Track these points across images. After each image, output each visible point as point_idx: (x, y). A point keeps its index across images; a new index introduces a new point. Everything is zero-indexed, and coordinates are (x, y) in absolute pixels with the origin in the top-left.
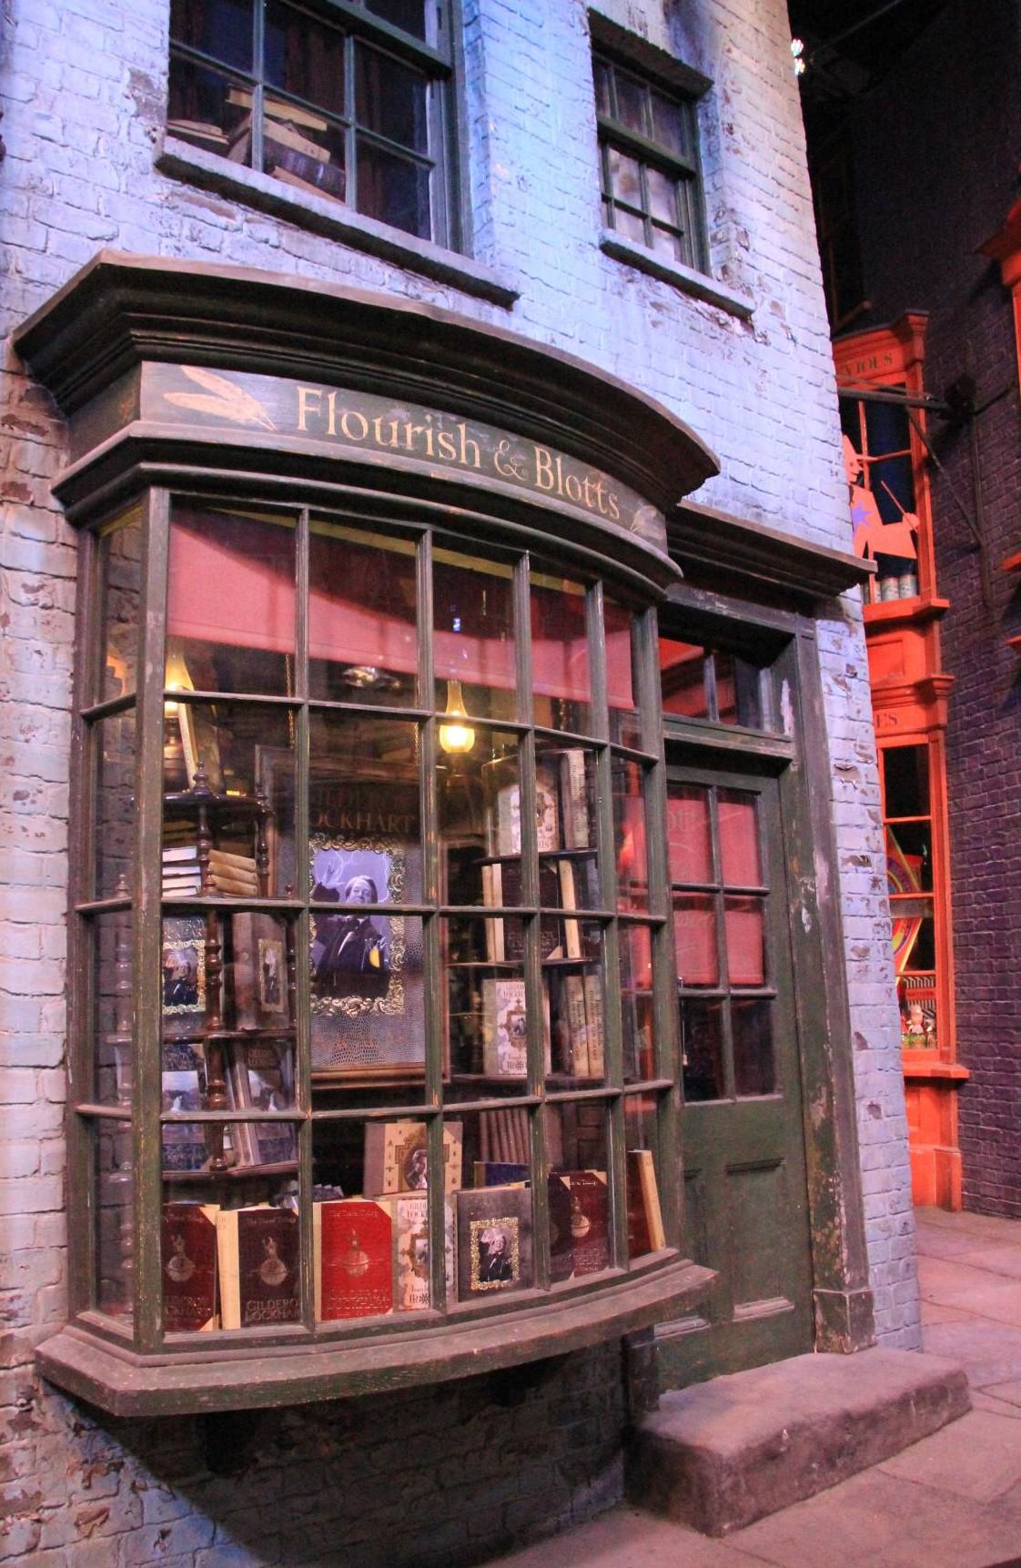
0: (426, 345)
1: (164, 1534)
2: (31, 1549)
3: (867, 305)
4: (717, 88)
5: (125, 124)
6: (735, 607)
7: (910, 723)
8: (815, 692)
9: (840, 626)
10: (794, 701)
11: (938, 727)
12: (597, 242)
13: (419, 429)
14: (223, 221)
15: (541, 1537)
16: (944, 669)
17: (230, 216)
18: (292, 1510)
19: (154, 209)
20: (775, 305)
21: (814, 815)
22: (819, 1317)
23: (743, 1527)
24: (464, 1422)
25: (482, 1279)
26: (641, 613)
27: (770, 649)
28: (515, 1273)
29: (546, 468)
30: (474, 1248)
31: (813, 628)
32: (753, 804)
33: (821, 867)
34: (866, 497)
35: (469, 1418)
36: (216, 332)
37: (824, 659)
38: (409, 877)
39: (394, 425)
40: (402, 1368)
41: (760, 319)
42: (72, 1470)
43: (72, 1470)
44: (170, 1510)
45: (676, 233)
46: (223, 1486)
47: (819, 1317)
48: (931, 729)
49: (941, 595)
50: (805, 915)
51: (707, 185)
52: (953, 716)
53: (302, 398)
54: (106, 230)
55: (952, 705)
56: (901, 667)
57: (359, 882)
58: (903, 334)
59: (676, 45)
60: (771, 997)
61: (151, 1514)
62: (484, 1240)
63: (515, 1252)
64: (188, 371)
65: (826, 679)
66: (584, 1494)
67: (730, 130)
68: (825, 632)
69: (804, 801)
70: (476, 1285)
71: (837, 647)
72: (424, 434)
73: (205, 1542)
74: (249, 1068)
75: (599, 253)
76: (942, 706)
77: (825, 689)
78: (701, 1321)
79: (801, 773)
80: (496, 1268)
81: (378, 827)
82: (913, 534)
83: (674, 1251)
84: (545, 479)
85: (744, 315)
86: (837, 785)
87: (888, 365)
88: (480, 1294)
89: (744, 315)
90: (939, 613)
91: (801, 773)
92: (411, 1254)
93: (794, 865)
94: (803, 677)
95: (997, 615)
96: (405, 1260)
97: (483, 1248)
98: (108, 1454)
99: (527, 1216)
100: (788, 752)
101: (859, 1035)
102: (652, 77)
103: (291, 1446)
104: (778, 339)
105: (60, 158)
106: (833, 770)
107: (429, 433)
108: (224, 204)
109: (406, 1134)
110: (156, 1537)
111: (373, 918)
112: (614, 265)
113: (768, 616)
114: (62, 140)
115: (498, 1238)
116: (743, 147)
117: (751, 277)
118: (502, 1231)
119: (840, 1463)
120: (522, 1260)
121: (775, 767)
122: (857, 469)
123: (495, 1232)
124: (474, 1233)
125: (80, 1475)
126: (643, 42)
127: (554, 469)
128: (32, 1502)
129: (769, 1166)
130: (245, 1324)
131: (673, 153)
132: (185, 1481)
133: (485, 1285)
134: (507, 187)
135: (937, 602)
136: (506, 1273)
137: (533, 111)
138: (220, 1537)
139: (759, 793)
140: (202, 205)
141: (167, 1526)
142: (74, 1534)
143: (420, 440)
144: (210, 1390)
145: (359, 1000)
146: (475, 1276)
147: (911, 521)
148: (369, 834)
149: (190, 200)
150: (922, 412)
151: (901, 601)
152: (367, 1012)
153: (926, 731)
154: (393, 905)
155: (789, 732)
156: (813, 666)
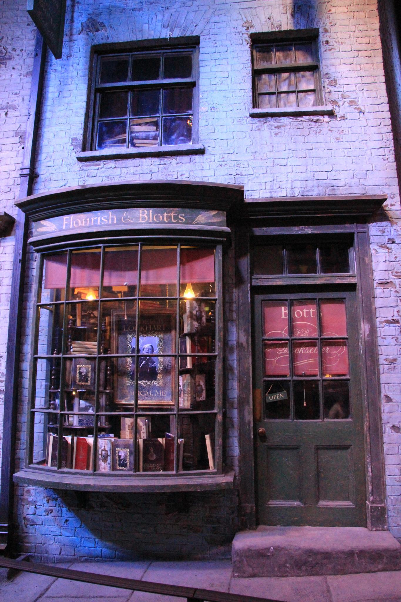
0: (86, 196)
1: (67, 520)
2: (34, 514)
5: (70, 153)
6: (315, 229)
9: (385, 223)
12: (248, 116)
13: (96, 218)
14: (97, 167)
15: (196, 559)
17: (99, 165)
18: (105, 525)
19: (79, 172)
23: (242, 577)
24: (166, 514)
25: (119, 466)
26: (215, 247)
27: (348, 241)
28: (128, 466)
29: (145, 215)
30: (117, 457)
31: (368, 227)
35: (168, 514)
36: (48, 209)
38: (164, 344)
39: (88, 219)
40: (70, 484)
42: (44, 498)
43: (44, 498)
44: (69, 514)
46: (83, 512)
53: (65, 220)
54: (63, 183)
57: (147, 346)
60: (349, 380)
61: (64, 515)
62: (120, 454)
63: (128, 459)
64: (42, 222)
66: (214, 550)
67: (327, 42)
70: (118, 468)
72: (97, 220)
73: (78, 526)
74: (80, 399)
75: (250, 119)
77: (373, 252)
78: (300, 503)
80: (123, 464)
81: (154, 329)
83: (215, 470)
84: (143, 218)
86: (378, 291)
88: (119, 470)
92: (101, 455)
96: (100, 457)
97: (119, 456)
98: (54, 496)
99: (132, 449)
101: (386, 396)
103: (104, 507)
105: (52, 170)
106: (375, 285)
107: (99, 218)
108: (98, 162)
109: (131, 422)
110: (64, 521)
111: (152, 358)
112: (257, 120)
113: (341, 228)
114: (53, 165)
115: (123, 454)
118: (124, 452)
119: (304, 568)
120: (130, 462)
123: (123, 452)
124: (117, 452)
125: (46, 499)
127: (148, 215)
128: (34, 503)
129: (346, 448)
130: (51, 466)
132: (73, 508)
133: (121, 468)
134: (207, 113)
136: (126, 466)
137: (220, 82)
138: (83, 525)
139: (345, 298)
140: (90, 166)
141: (68, 519)
142: (44, 514)
143: (96, 221)
144: (29, 479)
145: (146, 381)
146: (117, 465)
148: (151, 332)
149: (88, 166)
152: (149, 385)
154: (159, 354)
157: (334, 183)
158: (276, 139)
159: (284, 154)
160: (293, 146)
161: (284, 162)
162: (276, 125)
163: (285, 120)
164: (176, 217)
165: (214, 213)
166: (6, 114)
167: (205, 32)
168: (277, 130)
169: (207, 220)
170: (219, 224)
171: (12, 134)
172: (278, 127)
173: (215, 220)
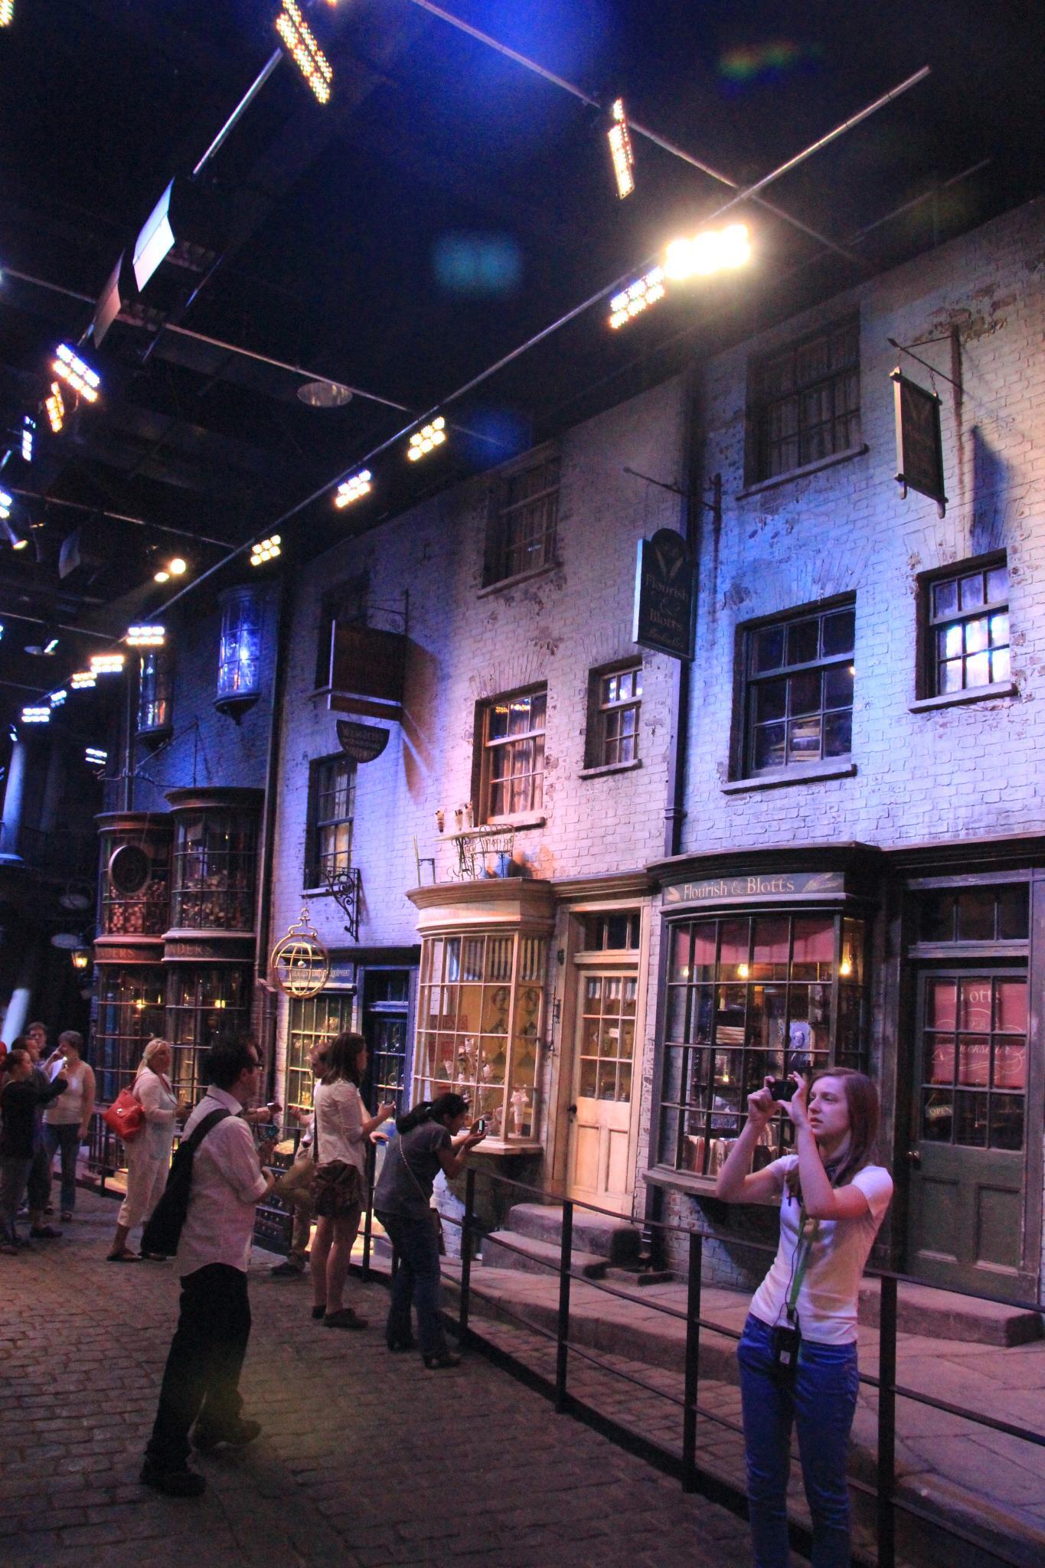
112: (919, 716)
157: (1007, 806)
158: (942, 745)
159: (948, 768)
160: (959, 755)
161: (946, 780)
162: (941, 721)
163: (954, 711)
164: (784, 886)
165: (828, 875)
166: (653, 732)
167: (863, 581)
168: (941, 730)
169: (820, 887)
170: (832, 890)
171: (660, 759)
172: (943, 725)
173: (830, 885)
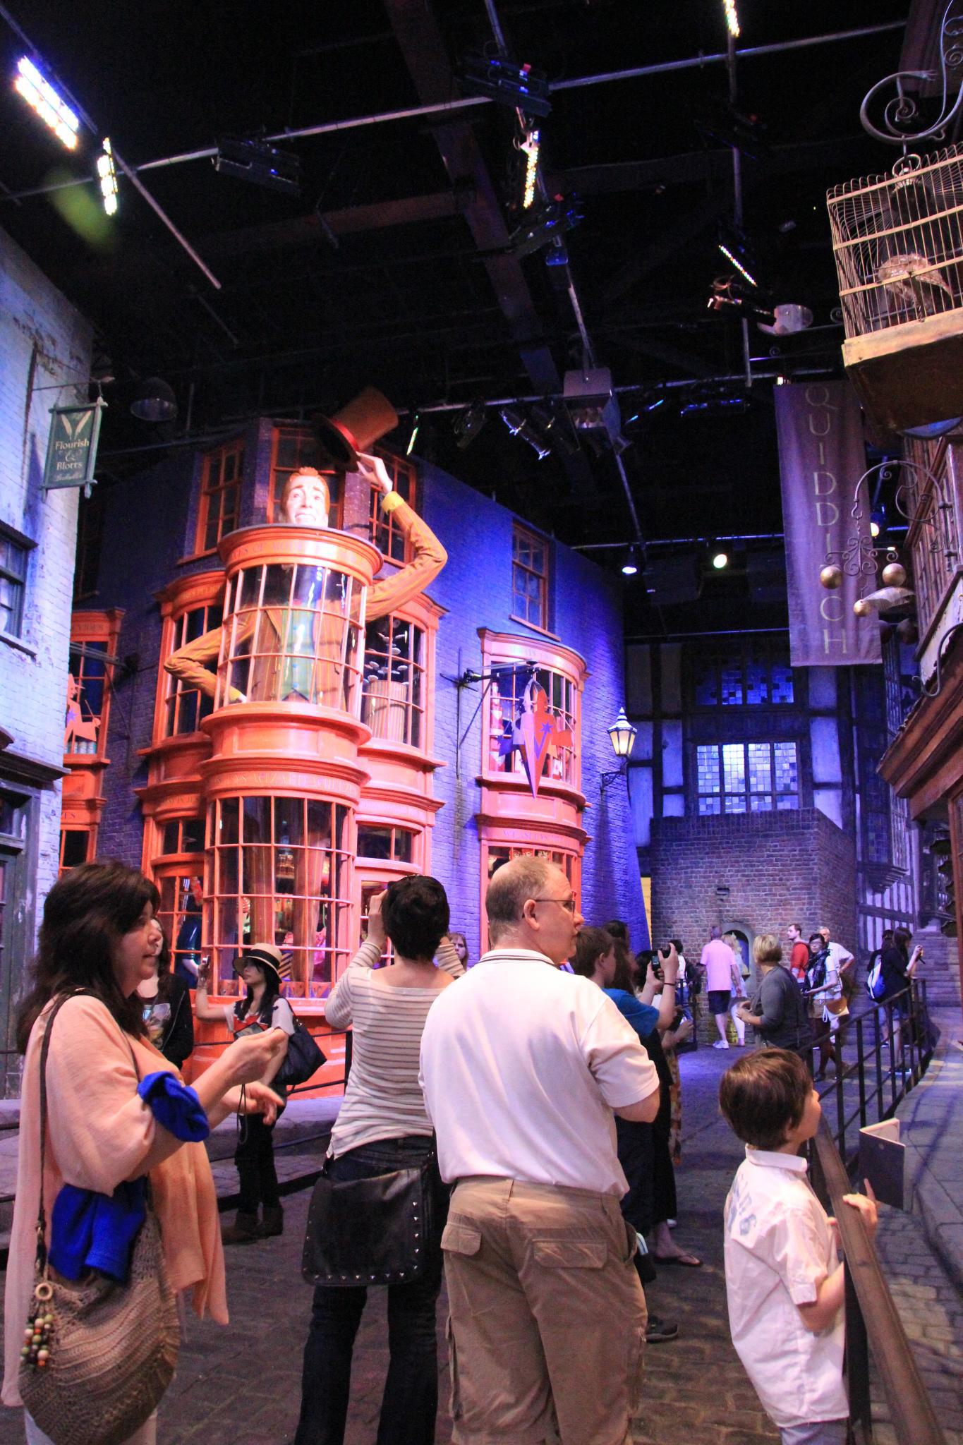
3: (97, 593)
4: (40, 547)
7: (81, 821)
8: (37, 822)
10: (27, 824)
11: (95, 823)
16: (103, 795)
20: (47, 649)
21: (29, 874)
22: (8, 1085)
27: (21, 801)
32: (4, 866)
33: (29, 895)
34: (76, 708)
37: (43, 808)
41: (38, 658)
45: (9, 609)
47: (8, 1085)
48: (92, 824)
49: (107, 756)
50: (20, 915)
51: (27, 591)
52: (104, 819)
55: (104, 813)
56: (81, 789)
58: (111, 617)
59: (26, 528)
65: (42, 816)
68: (45, 795)
69: (26, 866)
71: (49, 802)
76: (99, 813)
79: (26, 855)
82: (97, 730)
85: (32, 655)
86: (40, 861)
87: (101, 629)
89: (32, 655)
90: (105, 766)
91: (26, 855)
93: (18, 894)
94: (33, 814)
95: (132, 773)
100: (22, 846)
102: (11, 538)
104: (45, 664)
116: (46, 575)
117: (39, 636)
121: (16, 852)
122: (74, 692)
126: (12, 529)
131: (15, 575)
135: (105, 760)
147: (96, 722)
150: (113, 667)
151: (86, 756)
153: (90, 824)
155: (23, 837)
156: (38, 810)
